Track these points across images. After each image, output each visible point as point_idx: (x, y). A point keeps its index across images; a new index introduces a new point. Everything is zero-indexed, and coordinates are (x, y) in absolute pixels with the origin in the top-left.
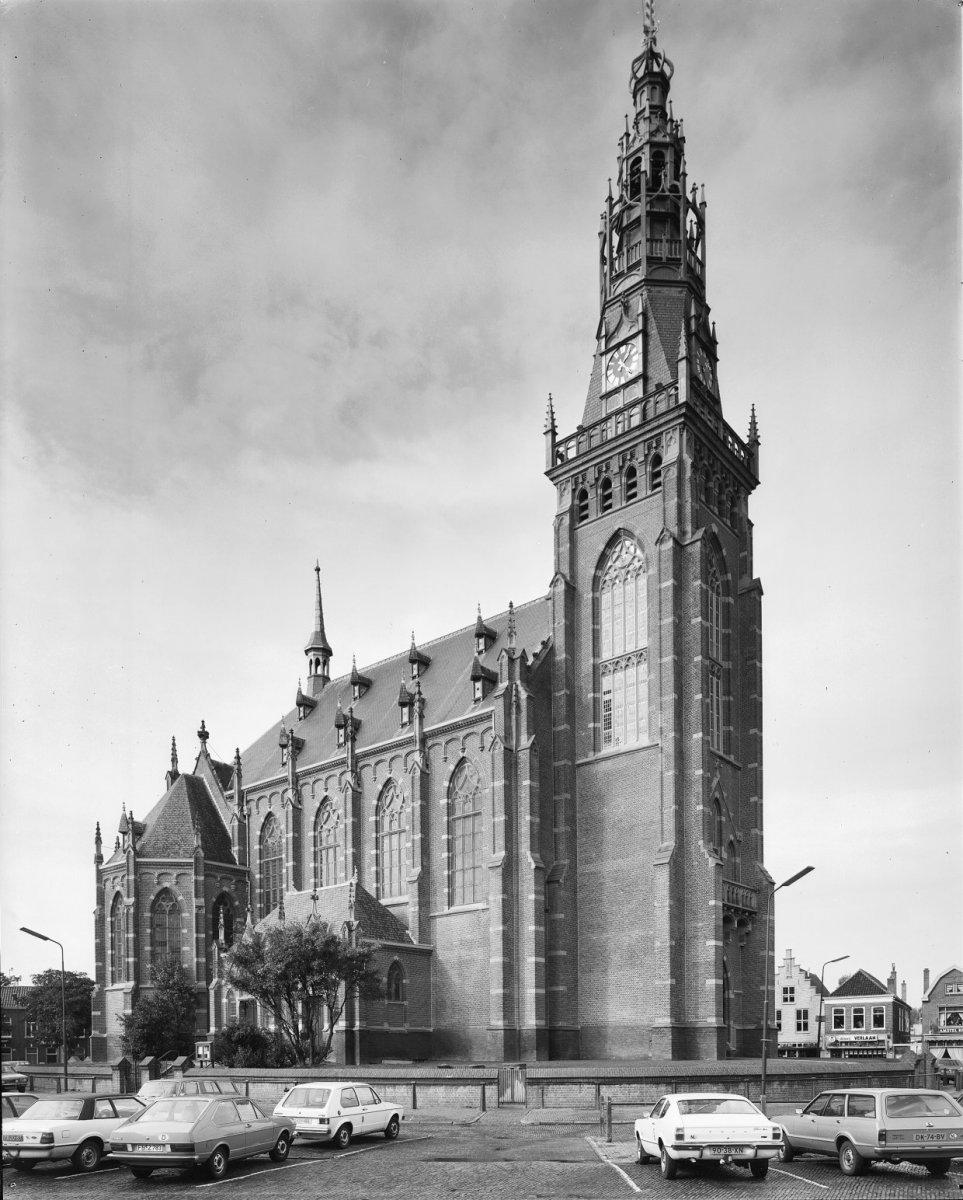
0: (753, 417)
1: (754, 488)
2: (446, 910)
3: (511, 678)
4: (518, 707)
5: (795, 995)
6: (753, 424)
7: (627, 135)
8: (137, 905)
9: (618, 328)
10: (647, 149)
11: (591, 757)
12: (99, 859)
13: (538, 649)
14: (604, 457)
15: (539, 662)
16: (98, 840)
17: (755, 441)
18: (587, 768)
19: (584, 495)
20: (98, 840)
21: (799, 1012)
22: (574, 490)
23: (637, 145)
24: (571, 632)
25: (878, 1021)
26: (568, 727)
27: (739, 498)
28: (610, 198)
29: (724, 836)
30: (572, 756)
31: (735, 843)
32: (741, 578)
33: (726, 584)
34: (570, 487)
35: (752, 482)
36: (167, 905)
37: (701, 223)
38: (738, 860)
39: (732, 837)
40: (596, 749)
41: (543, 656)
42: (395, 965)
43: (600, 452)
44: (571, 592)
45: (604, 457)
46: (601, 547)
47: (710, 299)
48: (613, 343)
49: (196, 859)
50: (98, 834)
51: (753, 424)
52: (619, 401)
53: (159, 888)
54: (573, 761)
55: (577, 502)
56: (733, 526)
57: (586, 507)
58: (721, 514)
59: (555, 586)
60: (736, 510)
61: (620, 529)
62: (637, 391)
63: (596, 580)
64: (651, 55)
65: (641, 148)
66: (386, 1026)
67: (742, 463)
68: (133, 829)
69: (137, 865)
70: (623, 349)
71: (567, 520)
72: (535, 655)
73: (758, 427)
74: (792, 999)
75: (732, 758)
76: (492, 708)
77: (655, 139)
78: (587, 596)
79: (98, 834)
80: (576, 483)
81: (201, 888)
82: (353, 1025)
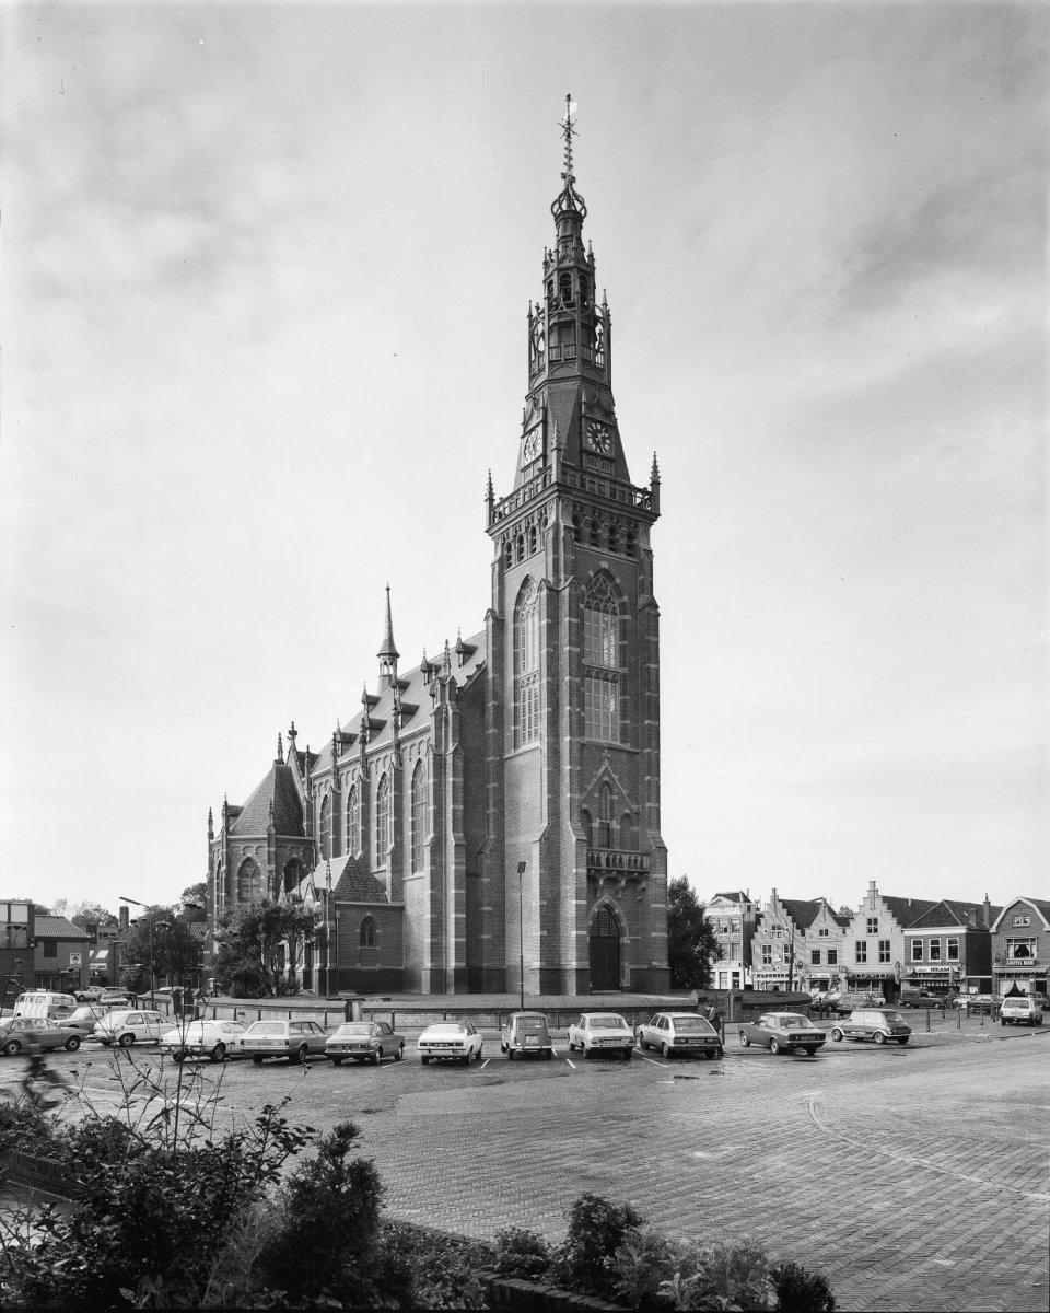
2: (411, 877)
5: (879, 926)
8: (229, 871)
9: (531, 418)
10: (556, 273)
12: (211, 835)
14: (517, 520)
16: (211, 821)
20: (211, 821)
21: (881, 943)
22: (503, 544)
24: (499, 655)
25: (953, 953)
26: (496, 731)
33: (623, 605)
36: (249, 870)
39: (627, 811)
42: (368, 920)
48: (528, 429)
49: (269, 834)
50: (210, 816)
53: (244, 858)
54: (501, 755)
55: (505, 553)
64: (569, 195)
65: (552, 274)
66: (358, 966)
68: (231, 813)
69: (228, 841)
70: (533, 433)
74: (876, 931)
77: (563, 265)
78: (510, 626)
79: (210, 816)
81: (273, 856)
82: (326, 966)
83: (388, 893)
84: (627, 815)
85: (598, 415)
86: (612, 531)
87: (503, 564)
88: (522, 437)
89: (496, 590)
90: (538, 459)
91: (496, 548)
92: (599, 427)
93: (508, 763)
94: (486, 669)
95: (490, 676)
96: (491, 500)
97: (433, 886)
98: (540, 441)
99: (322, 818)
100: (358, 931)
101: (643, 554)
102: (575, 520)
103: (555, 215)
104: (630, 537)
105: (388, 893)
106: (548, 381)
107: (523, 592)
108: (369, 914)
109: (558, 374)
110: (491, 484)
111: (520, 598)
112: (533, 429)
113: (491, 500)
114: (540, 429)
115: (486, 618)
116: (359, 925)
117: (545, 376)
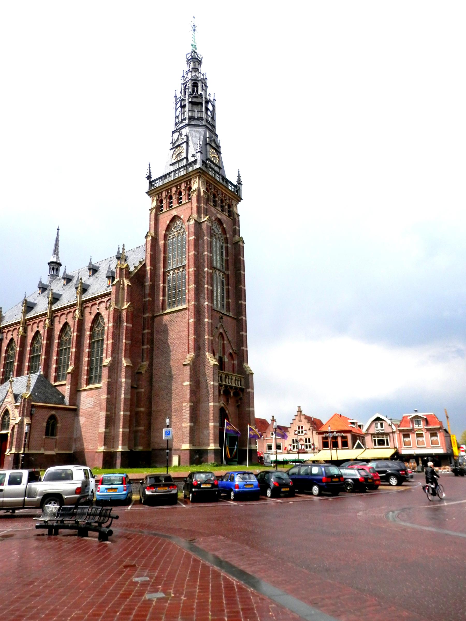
0: (239, 174)
1: (240, 201)
2: (85, 388)
3: (121, 276)
4: (123, 289)
6: (239, 177)
7: (183, 76)
11: (161, 313)
13: (137, 264)
15: (136, 271)
17: (240, 183)
18: (158, 318)
19: (161, 202)
22: (157, 200)
23: (187, 80)
26: (151, 299)
27: (232, 205)
28: (176, 96)
29: (226, 350)
30: (153, 311)
31: (233, 354)
32: (234, 236)
34: (156, 198)
35: (239, 199)
37: (214, 106)
38: (235, 362)
39: (231, 351)
40: (163, 309)
41: (139, 267)
43: (167, 185)
44: (155, 241)
45: (169, 187)
46: (168, 222)
47: (218, 131)
51: (239, 177)
52: (178, 166)
55: (159, 204)
56: (229, 216)
57: (162, 207)
58: (222, 211)
59: (147, 238)
60: (231, 209)
61: (175, 215)
62: (184, 162)
63: (165, 236)
65: (188, 81)
67: (233, 192)
70: (179, 148)
71: (154, 211)
72: (135, 267)
73: (241, 178)
75: (231, 314)
76: (111, 290)
78: (161, 242)
80: (159, 197)
83: (67, 400)
84: (230, 354)
85: (213, 145)
86: (222, 201)
87: (158, 209)
88: (171, 149)
89: (153, 223)
90: (183, 159)
91: (152, 202)
92: (214, 151)
93: (156, 319)
94: (145, 264)
95: (148, 268)
96: (149, 177)
97: (109, 393)
98: (185, 151)
99: (31, 346)
100: (45, 424)
101: (236, 216)
102: (207, 189)
103: (187, 59)
104: (230, 206)
105: (67, 400)
106: (188, 125)
107: (171, 224)
108: (53, 412)
109: (193, 123)
110: (150, 170)
111: (168, 228)
112: (179, 146)
113: (149, 177)
114: (184, 146)
115: (146, 237)
116: (46, 420)
117: (187, 122)
